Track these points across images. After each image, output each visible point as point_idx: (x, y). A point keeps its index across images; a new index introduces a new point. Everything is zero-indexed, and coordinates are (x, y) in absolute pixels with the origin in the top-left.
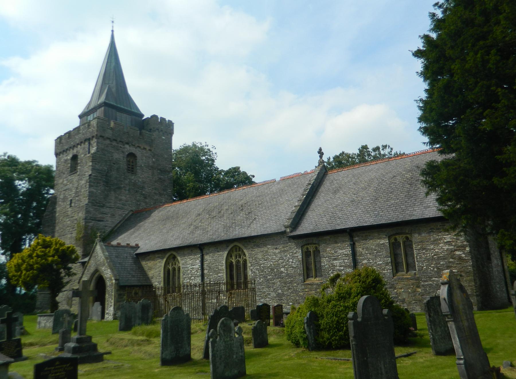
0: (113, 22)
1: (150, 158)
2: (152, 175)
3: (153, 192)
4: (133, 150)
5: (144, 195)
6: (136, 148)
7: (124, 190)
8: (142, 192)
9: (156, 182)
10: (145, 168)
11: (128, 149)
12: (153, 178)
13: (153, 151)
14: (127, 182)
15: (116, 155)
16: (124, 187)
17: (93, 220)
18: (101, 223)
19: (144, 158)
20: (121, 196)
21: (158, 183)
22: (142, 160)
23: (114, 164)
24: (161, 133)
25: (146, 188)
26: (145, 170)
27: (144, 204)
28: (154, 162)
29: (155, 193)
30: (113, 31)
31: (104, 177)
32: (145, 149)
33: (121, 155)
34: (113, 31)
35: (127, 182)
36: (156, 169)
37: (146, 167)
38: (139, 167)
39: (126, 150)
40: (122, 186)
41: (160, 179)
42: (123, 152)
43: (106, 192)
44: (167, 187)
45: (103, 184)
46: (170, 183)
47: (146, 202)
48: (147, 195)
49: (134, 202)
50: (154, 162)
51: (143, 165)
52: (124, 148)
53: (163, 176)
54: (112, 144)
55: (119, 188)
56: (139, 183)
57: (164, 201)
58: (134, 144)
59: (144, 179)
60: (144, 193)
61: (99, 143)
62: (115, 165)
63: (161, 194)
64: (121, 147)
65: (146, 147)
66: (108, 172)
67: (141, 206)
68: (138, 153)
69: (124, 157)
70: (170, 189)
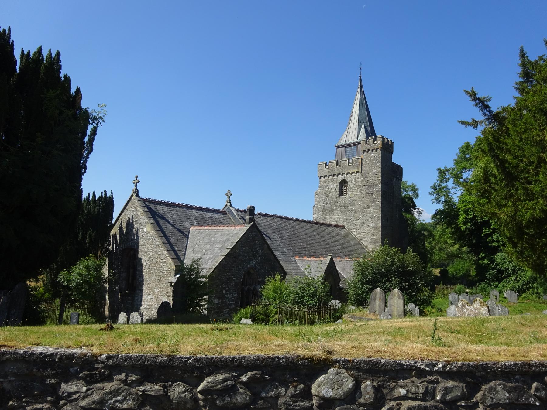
0: (360, 68)
1: (358, 178)
6: (347, 174)
8: (352, 209)
11: (341, 178)
16: (336, 209)
19: (354, 180)
23: (329, 193)
24: (370, 152)
28: (362, 181)
29: (363, 207)
32: (353, 173)
35: (338, 204)
43: (324, 216)
50: (362, 181)
56: (349, 202)
67: (351, 220)
68: (348, 178)
70: (378, 200)
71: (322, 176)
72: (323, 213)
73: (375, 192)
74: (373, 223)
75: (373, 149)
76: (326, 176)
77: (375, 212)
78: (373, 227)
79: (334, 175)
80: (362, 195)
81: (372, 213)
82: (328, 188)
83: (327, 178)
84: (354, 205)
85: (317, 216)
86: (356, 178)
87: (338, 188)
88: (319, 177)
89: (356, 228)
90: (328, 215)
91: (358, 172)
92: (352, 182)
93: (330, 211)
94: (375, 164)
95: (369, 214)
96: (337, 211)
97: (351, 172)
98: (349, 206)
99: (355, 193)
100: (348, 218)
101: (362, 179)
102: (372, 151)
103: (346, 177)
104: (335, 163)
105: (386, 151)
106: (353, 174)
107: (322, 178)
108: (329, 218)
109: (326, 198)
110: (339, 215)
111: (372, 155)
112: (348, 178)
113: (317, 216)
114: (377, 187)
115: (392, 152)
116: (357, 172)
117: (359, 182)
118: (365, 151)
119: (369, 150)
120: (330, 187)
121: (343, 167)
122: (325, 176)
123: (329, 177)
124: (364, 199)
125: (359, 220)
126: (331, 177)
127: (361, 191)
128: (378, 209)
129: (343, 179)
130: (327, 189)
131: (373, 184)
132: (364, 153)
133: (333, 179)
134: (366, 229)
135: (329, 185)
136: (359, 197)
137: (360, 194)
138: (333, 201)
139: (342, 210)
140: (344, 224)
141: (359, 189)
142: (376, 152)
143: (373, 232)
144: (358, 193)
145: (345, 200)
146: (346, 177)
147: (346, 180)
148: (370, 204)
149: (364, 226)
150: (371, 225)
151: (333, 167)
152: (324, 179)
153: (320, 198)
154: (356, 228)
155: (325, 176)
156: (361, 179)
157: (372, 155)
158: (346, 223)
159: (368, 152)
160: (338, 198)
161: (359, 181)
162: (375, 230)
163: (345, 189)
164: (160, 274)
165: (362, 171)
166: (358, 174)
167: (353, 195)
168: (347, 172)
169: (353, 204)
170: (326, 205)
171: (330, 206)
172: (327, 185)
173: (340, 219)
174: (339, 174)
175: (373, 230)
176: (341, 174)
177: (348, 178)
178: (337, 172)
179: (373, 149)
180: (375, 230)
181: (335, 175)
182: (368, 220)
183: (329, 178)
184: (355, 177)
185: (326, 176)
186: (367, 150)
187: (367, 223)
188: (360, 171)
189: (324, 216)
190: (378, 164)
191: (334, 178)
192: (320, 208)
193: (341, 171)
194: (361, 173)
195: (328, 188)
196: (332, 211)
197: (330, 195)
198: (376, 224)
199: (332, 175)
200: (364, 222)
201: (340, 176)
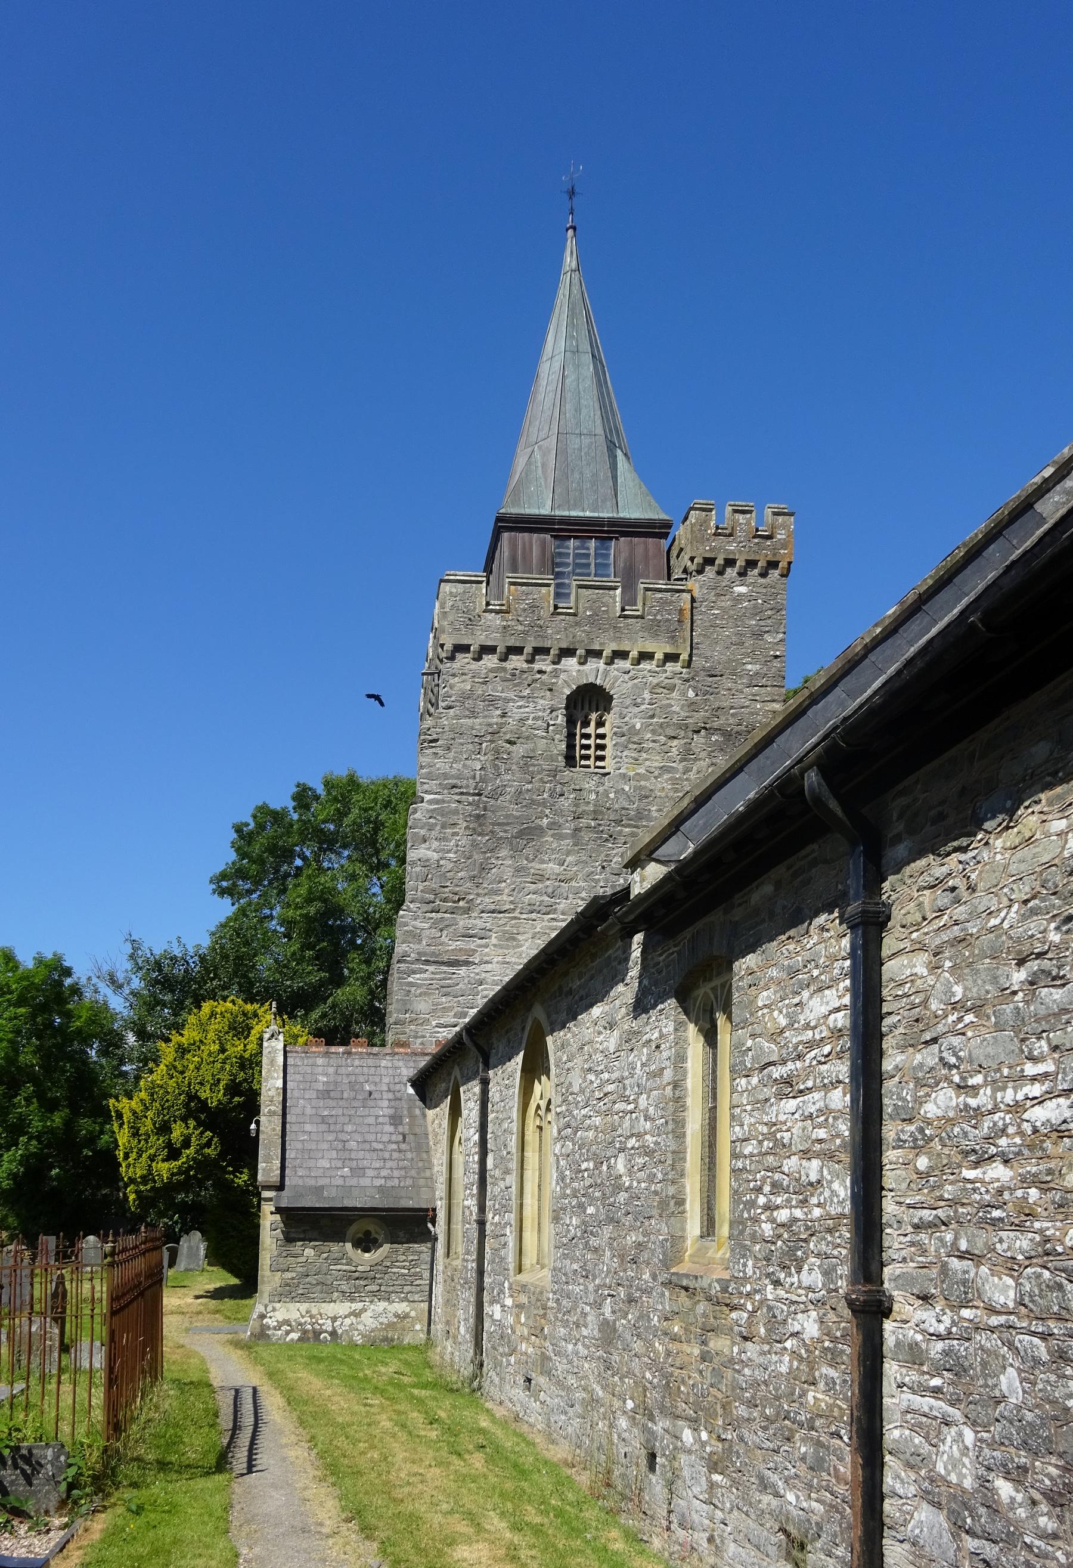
1: (671, 688)
4: (594, 672)
6: (610, 662)
10: (649, 735)
12: (687, 770)
15: (520, 707)
16: (552, 825)
17: (427, 963)
18: (462, 971)
19: (647, 695)
20: (543, 862)
24: (731, 573)
26: (651, 745)
28: (692, 706)
31: (471, 799)
33: (542, 702)
35: (565, 803)
36: (703, 732)
37: (653, 732)
39: (563, 676)
40: (545, 821)
42: (550, 690)
43: (478, 857)
45: (467, 828)
49: (597, 881)
50: (692, 706)
51: (638, 726)
52: (556, 674)
54: (504, 669)
58: (596, 647)
59: (643, 783)
62: (514, 748)
64: (540, 672)
71: (465, 648)
72: (474, 845)
75: (751, 564)
76: (491, 650)
83: (490, 661)
85: (436, 856)
88: (448, 647)
90: (503, 853)
92: (636, 705)
93: (521, 834)
94: (758, 635)
96: (560, 837)
97: (634, 654)
98: (619, 822)
99: (656, 761)
101: (691, 694)
102: (742, 574)
103: (606, 673)
104: (544, 590)
106: (645, 665)
107: (462, 659)
108: (508, 873)
109: (496, 767)
110: (570, 859)
111: (743, 589)
112: (616, 679)
113: (436, 856)
119: (730, 562)
120: (516, 711)
121: (593, 621)
122: (487, 650)
123: (504, 659)
126: (516, 662)
127: (687, 754)
129: (591, 680)
133: (531, 670)
135: (507, 700)
136: (674, 781)
137: (680, 767)
138: (537, 785)
139: (586, 836)
141: (675, 742)
142: (762, 581)
145: (601, 789)
146: (606, 673)
147: (607, 687)
151: (533, 607)
152: (475, 665)
153: (455, 760)
155: (487, 650)
157: (743, 589)
159: (720, 573)
161: (676, 703)
166: (670, 666)
167: (642, 771)
168: (614, 646)
170: (492, 802)
171: (515, 811)
172: (500, 698)
173: (573, 884)
174: (568, 652)
176: (580, 652)
177: (616, 679)
178: (557, 639)
179: (751, 564)
181: (546, 651)
184: (655, 681)
185: (491, 650)
186: (720, 561)
188: (684, 656)
189: (478, 857)
190: (769, 638)
191: (537, 666)
192: (456, 812)
193: (580, 634)
194: (689, 664)
196: (529, 833)
197: (519, 750)
199: (528, 650)
201: (570, 663)
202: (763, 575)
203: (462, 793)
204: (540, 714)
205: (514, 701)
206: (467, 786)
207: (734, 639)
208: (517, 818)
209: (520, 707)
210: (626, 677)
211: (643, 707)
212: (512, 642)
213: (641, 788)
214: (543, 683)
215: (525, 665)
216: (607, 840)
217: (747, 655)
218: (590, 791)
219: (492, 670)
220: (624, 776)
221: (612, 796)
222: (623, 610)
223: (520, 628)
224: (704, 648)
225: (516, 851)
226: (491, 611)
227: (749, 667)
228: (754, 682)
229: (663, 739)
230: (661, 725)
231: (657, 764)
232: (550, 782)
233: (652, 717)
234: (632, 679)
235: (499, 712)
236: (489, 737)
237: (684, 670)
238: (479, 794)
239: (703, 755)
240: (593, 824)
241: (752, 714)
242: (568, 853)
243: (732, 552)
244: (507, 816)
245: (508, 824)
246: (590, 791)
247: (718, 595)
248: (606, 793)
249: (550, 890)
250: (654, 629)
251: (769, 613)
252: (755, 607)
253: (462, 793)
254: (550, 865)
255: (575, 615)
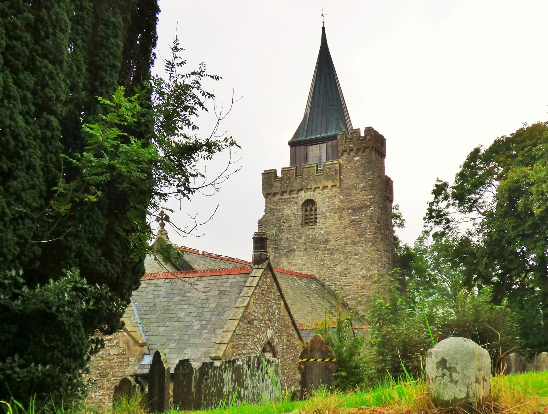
0: (323, 15)
1: (335, 196)
2: (340, 220)
3: (343, 242)
5: (328, 250)
7: (299, 251)
8: (326, 247)
9: (346, 228)
10: (328, 213)
12: (341, 223)
13: (338, 185)
14: (302, 240)
15: (287, 210)
16: (298, 248)
19: (327, 200)
21: (350, 227)
22: (324, 203)
23: (284, 223)
24: (352, 154)
25: (332, 240)
27: (329, 263)
30: (323, 28)
32: (325, 187)
34: (323, 28)
35: (302, 240)
37: (330, 212)
38: (320, 214)
40: (296, 247)
41: (353, 221)
42: (296, 203)
44: (365, 230)
45: (272, 252)
46: (369, 222)
47: (332, 260)
48: (333, 249)
50: (342, 201)
52: (298, 197)
53: (357, 215)
54: (282, 199)
55: (291, 251)
56: (321, 237)
57: (360, 251)
58: (309, 187)
59: (327, 230)
60: (328, 247)
61: (268, 203)
63: (355, 243)
64: (293, 198)
65: (326, 184)
66: (276, 236)
67: (326, 266)
68: (317, 196)
69: (297, 210)
73: (365, 220)
74: (363, 270)
77: (365, 251)
78: (363, 277)
79: (291, 191)
80: (343, 225)
81: (361, 254)
82: (282, 214)
83: (278, 197)
84: (330, 241)
86: (330, 196)
87: (300, 213)
89: (335, 279)
91: (335, 186)
93: (289, 252)
95: (356, 255)
96: (300, 251)
98: (320, 244)
99: (331, 222)
100: (319, 262)
103: (314, 195)
104: (292, 171)
105: (377, 154)
114: (368, 211)
115: (382, 155)
116: (332, 186)
117: (336, 203)
118: (345, 151)
119: (352, 150)
123: (282, 195)
124: (347, 230)
125: (340, 265)
126: (286, 196)
127: (341, 218)
128: (371, 247)
129: (309, 198)
130: (281, 216)
131: (360, 206)
132: (342, 155)
134: (351, 280)
135: (283, 209)
137: (339, 222)
140: (313, 273)
141: (336, 215)
142: (363, 154)
143: (363, 284)
144: (336, 221)
147: (314, 199)
148: (358, 239)
149: (348, 275)
150: (361, 273)
154: (335, 279)
156: (339, 197)
158: (316, 271)
159: (349, 154)
160: (302, 230)
161: (337, 201)
162: (366, 280)
163: (312, 215)
164: (102, 363)
165: (340, 184)
166: (334, 190)
167: (327, 225)
168: (315, 186)
169: (327, 241)
172: (280, 209)
173: (307, 266)
174: (301, 190)
175: (363, 281)
177: (317, 196)
180: (366, 280)
182: (354, 265)
183: (283, 197)
184: (329, 195)
185: (278, 193)
186: (348, 151)
187: (353, 270)
188: (338, 185)
191: (292, 196)
195: (282, 214)
197: (287, 225)
198: (368, 270)
199: (288, 191)
200: (347, 269)
201: (302, 193)
202: (364, 152)
203: (270, 241)
204: (293, 212)
205: (285, 209)
206: (272, 239)
207: (355, 176)
208: (287, 247)
209: (287, 210)
210: (320, 195)
211: (326, 204)
212: (283, 190)
213: (327, 231)
214: (294, 202)
215: (288, 196)
216: (316, 250)
217: (360, 180)
218: (310, 235)
219: (279, 200)
220: (321, 228)
221: (317, 235)
222: (317, 173)
223: (286, 185)
224: (345, 181)
225: (287, 256)
226: (277, 181)
227: (361, 185)
228: (363, 190)
229: (332, 214)
230: (332, 209)
231: (331, 223)
232: (297, 234)
233: (329, 207)
234: (322, 195)
235: (281, 213)
236: (277, 222)
237: (339, 190)
238: (275, 241)
239: (346, 217)
240: (311, 245)
241: (363, 200)
242: (304, 256)
243: (352, 147)
244: (284, 247)
245: (284, 249)
246: (310, 235)
247: (349, 162)
248: (315, 235)
249: (299, 269)
250: (327, 178)
251: (367, 165)
252: (362, 163)
253: (270, 241)
254: (299, 260)
255: (302, 178)
